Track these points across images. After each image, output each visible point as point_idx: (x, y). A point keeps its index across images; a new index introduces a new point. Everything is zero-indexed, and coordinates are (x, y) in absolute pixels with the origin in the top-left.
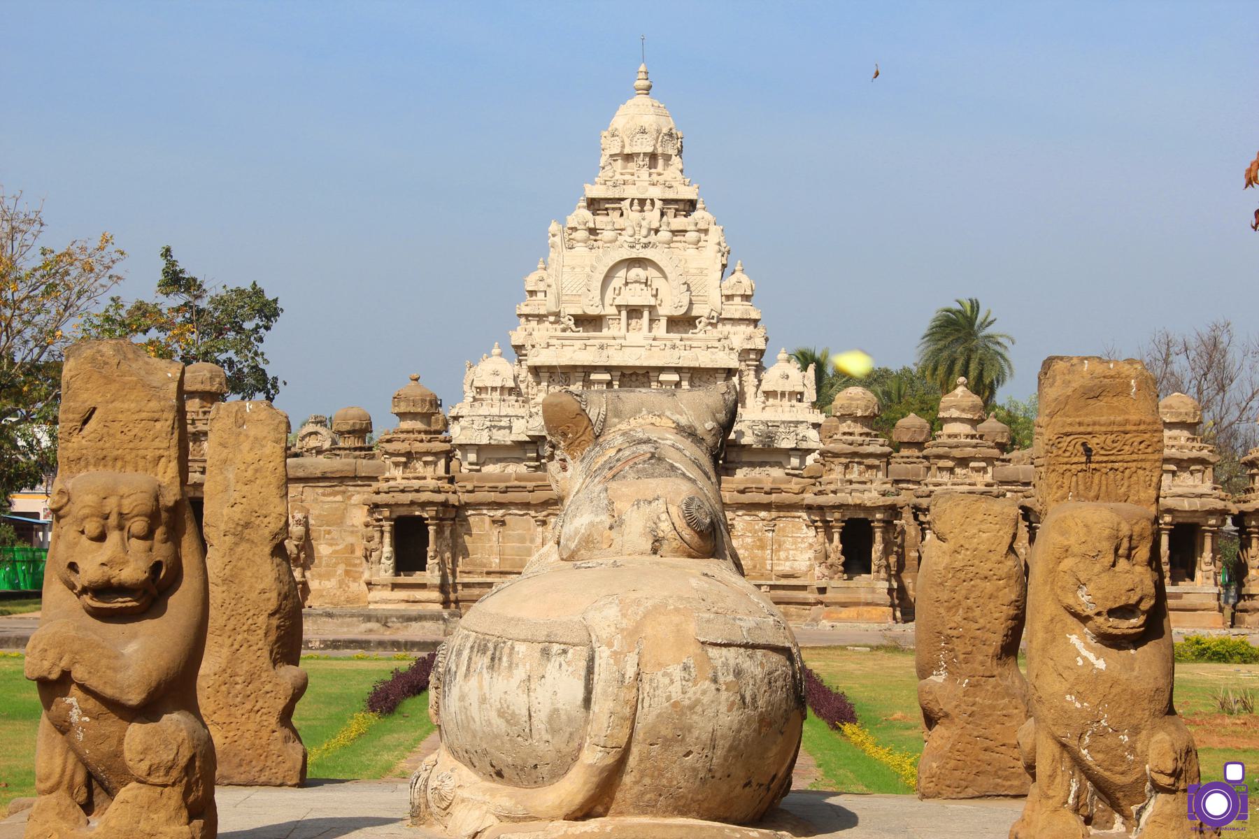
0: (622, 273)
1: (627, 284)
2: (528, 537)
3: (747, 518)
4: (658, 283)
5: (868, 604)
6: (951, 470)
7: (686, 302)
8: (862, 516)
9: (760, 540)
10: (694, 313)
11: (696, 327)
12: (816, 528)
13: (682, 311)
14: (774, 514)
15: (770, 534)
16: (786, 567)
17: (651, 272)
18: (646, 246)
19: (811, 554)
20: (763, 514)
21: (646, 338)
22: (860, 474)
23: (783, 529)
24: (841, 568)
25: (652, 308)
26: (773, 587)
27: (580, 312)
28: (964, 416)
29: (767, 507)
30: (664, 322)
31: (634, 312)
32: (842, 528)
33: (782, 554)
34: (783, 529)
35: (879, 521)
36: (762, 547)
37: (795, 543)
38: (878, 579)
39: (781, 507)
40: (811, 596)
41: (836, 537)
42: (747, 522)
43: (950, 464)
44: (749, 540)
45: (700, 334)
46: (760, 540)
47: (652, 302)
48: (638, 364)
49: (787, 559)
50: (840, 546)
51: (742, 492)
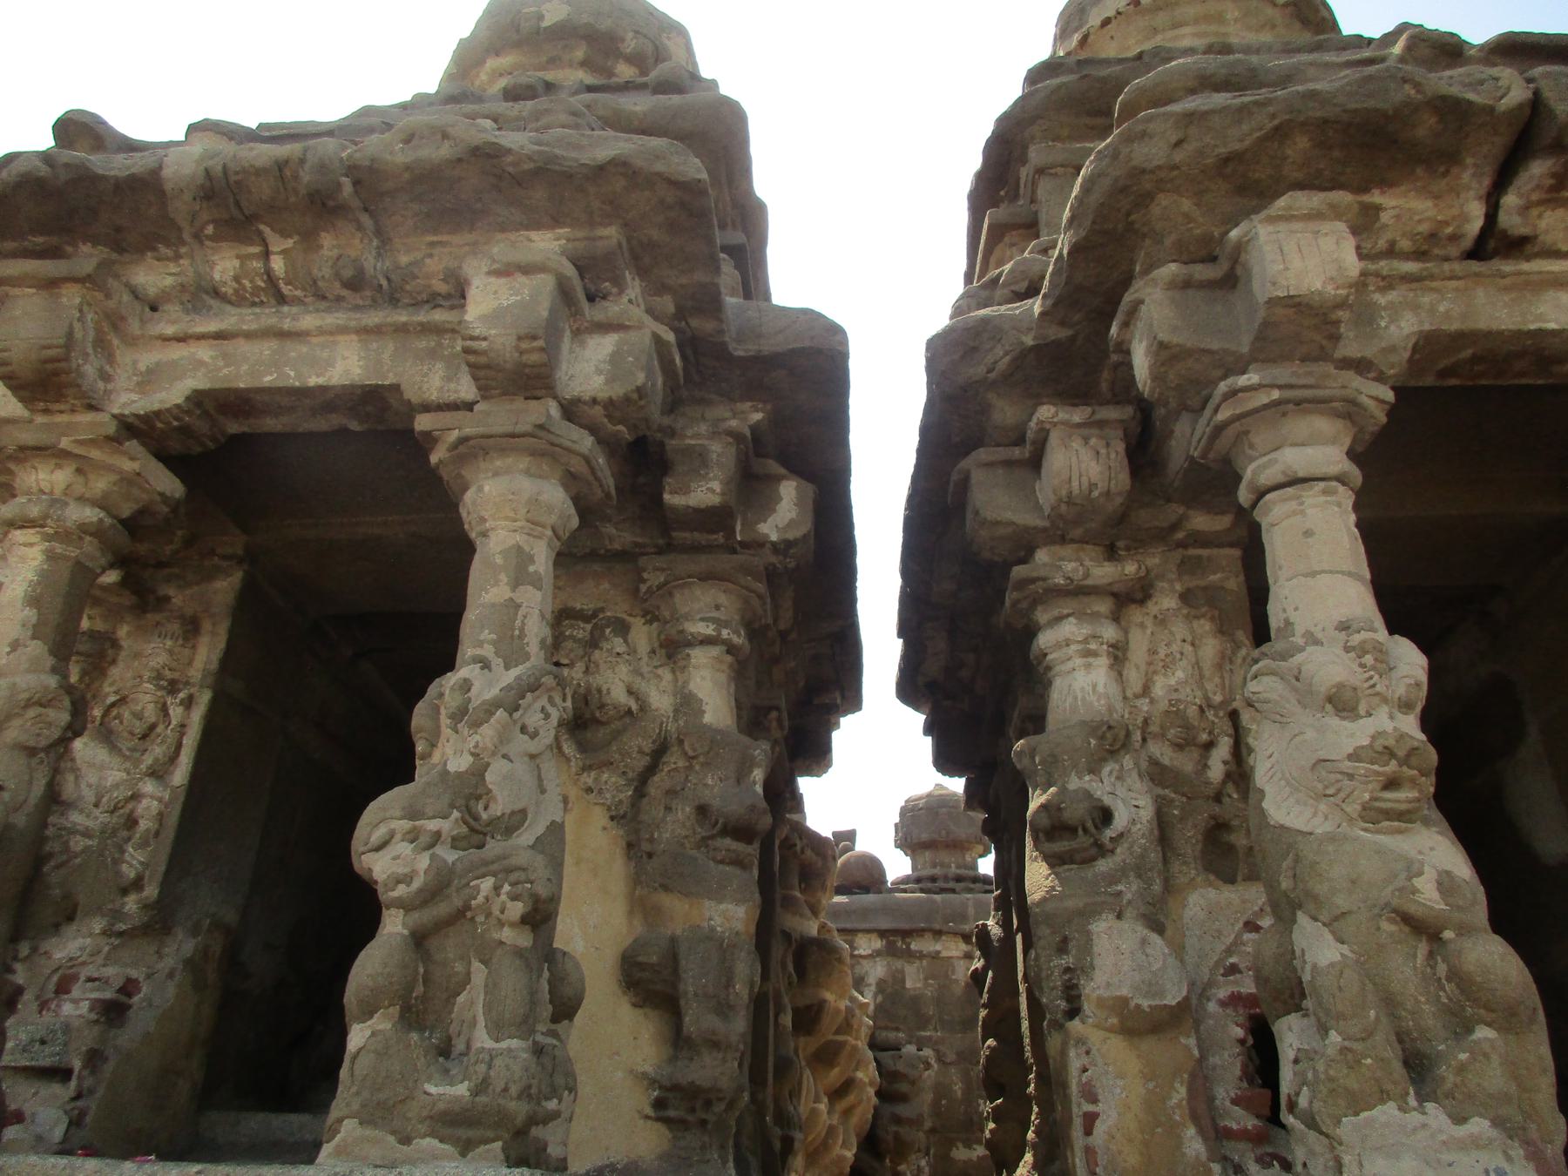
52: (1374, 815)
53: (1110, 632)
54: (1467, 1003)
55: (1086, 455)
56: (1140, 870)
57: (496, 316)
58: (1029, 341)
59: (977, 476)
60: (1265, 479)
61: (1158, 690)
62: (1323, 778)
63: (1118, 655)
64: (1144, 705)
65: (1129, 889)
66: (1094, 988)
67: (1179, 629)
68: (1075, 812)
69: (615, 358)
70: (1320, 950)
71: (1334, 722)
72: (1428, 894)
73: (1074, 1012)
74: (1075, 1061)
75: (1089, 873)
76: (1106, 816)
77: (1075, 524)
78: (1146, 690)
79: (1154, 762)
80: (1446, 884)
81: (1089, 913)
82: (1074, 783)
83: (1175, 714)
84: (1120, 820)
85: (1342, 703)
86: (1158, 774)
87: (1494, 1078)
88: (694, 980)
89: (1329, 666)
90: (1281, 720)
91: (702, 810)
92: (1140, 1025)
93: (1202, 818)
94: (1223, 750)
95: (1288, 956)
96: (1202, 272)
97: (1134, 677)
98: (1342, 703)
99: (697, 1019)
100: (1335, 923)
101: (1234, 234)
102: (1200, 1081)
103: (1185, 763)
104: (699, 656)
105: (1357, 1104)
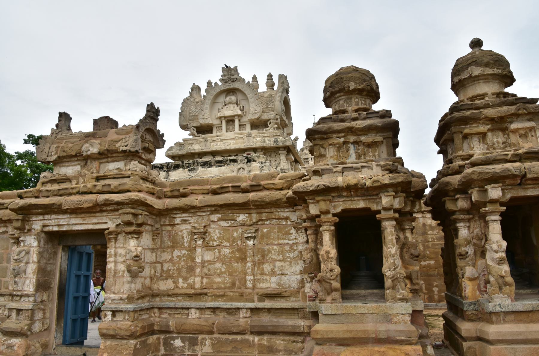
0: (222, 99)
1: (226, 105)
2: (5, 256)
3: (224, 224)
4: (243, 103)
5: (379, 341)
6: (483, 136)
7: (259, 109)
8: (362, 205)
9: (240, 250)
10: (265, 117)
11: (268, 127)
12: (306, 230)
13: (256, 116)
14: (255, 217)
15: (251, 243)
16: (271, 284)
17: (240, 97)
18: (233, 81)
19: (299, 267)
20: (242, 217)
21: (235, 134)
22: (359, 157)
23: (267, 236)
24: (336, 284)
25: (239, 116)
26: (254, 310)
27: (199, 125)
28: (489, 71)
29: (244, 207)
30: (248, 127)
31: (230, 121)
32: (336, 225)
33: (267, 267)
34: (267, 236)
35: (386, 209)
36: (243, 259)
37: (282, 252)
38: (395, 299)
39: (261, 206)
40: (301, 323)
41: (327, 238)
42: (224, 229)
43: (482, 128)
44: (227, 251)
45: (271, 130)
46: (240, 250)
47: (240, 113)
48: (228, 148)
49: (273, 273)
50: (333, 253)
51: (215, 192)
52: (499, 264)
53: (468, 225)
54: (506, 284)
55: (465, 203)
56: (472, 260)
57: (387, 202)
58: (456, 187)
59: (447, 201)
60: (489, 220)
61: (475, 232)
62: (493, 260)
63: (469, 228)
64: (473, 234)
65: (470, 263)
66: (466, 275)
67: (478, 222)
68: (464, 253)
69: (399, 202)
70: (492, 279)
71: (495, 254)
72: (503, 273)
73: (463, 278)
74: (463, 284)
75: (465, 261)
76: (467, 253)
77: (463, 211)
78: (473, 232)
79: (474, 243)
80: (506, 272)
81: (465, 266)
82: (463, 249)
83: (477, 235)
84: (469, 253)
85: (496, 252)
86: (475, 245)
87: (508, 291)
88: (414, 276)
89: (495, 247)
90: (490, 251)
91: (411, 254)
92: (471, 280)
93: (481, 251)
94: (484, 241)
95: (488, 278)
96: (481, 189)
97: (471, 230)
98: (496, 252)
99: (415, 281)
100: (493, 276)
101: (486, 187)
102: (479, 285)
103: (478, 242)
104: (407, 231)
105: (494, 294)
